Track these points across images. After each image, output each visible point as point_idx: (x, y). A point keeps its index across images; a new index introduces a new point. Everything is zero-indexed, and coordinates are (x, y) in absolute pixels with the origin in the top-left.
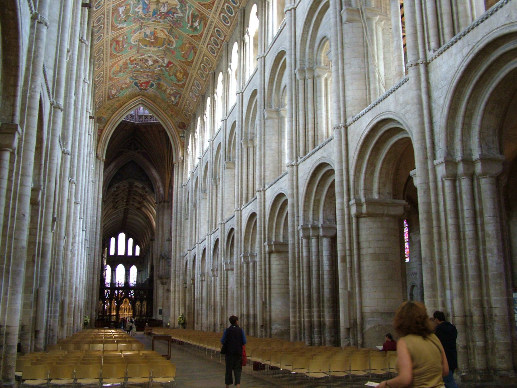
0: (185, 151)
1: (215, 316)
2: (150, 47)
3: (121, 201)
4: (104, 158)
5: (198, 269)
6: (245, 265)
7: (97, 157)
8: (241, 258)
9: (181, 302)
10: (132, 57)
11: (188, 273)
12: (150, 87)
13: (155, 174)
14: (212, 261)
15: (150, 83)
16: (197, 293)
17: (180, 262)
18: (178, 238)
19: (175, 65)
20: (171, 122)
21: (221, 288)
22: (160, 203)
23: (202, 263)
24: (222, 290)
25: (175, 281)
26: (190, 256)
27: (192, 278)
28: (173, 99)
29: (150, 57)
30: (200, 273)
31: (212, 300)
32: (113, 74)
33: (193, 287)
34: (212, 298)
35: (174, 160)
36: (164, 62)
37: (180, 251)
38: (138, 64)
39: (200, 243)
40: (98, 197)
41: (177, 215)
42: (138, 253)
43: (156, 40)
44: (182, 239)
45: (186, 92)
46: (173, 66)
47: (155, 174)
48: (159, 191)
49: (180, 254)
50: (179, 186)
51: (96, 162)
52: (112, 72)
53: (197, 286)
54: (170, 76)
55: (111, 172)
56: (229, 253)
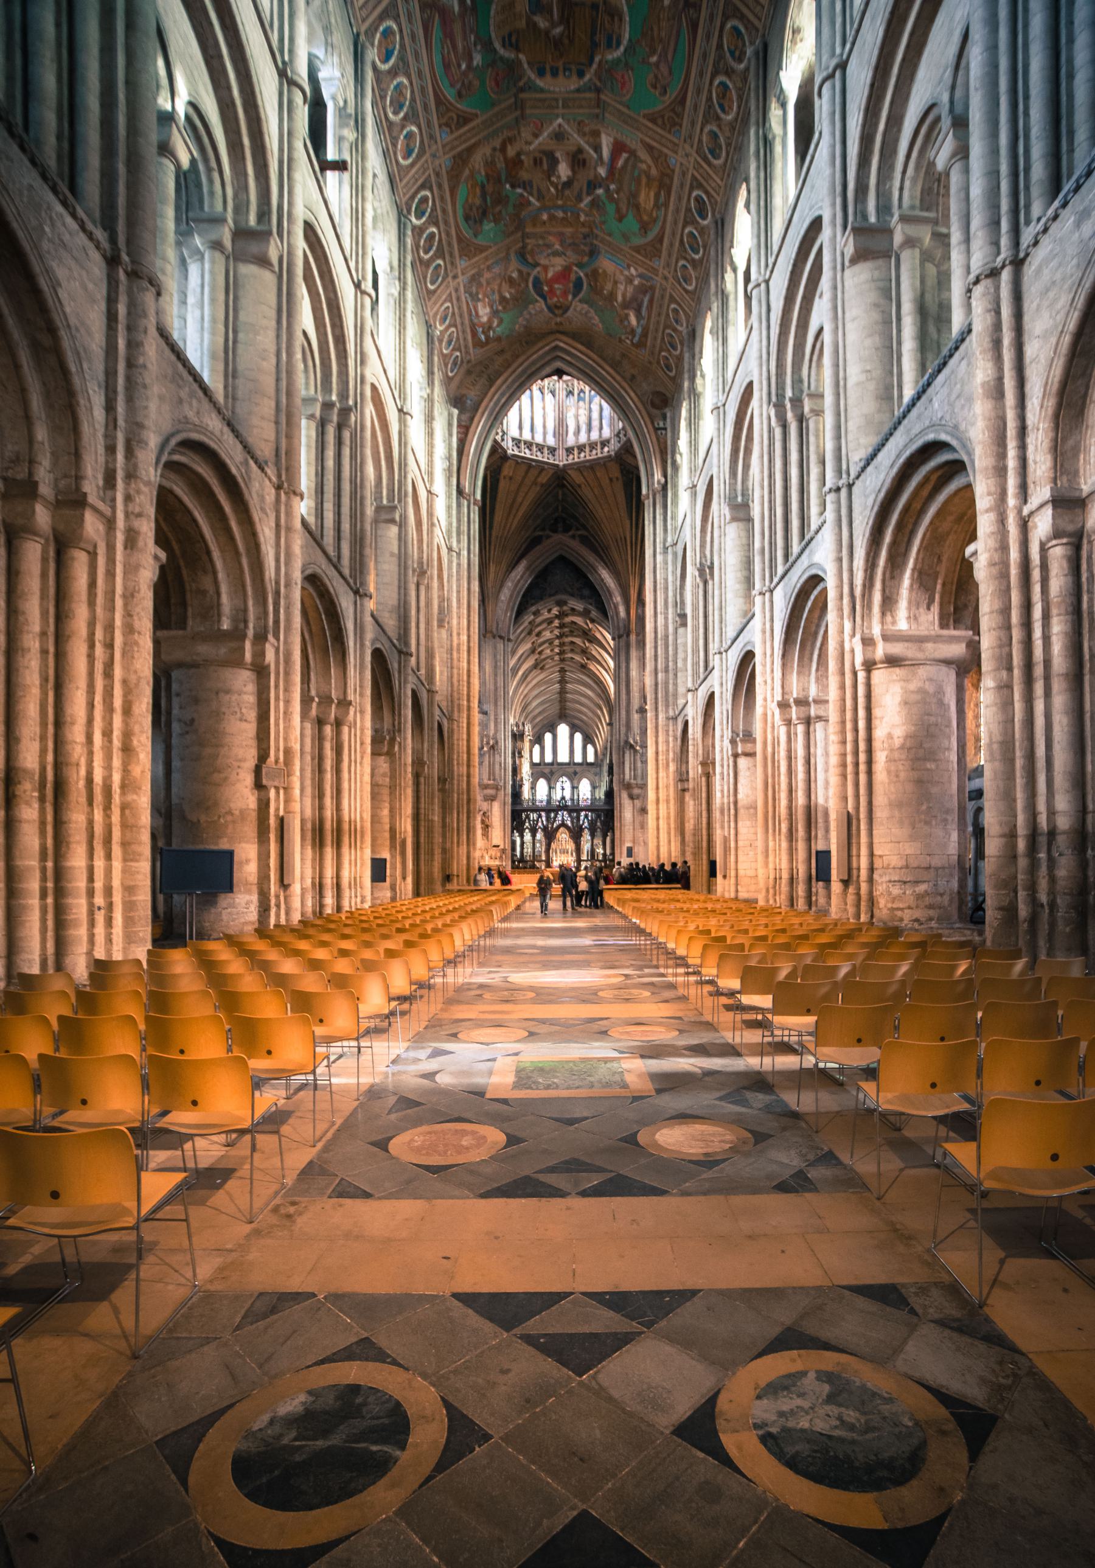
0: (669, 461)
1: (791, 851)
2: (555, 73)
3: (548, 651)
4: (479, 497)
5: (722, 724)
6: (1058, 553)
7: (460, 492)
8: (1024, 525)
9: (672, 826)
10: (511, 140)
11: (691, 748)
12: (575, 296)
13: (607, 577)
14: (778, 674)
15: (573, 277)
16: (722, 791)
17: (667, 731)
18: (660, 675)
19: (633, 153)
20: (632, 394)
21: (844, 742)
22: (620, 637)
23: (733, 705)
24: (849, 747)
25: (657, 778)
26: (695, 704)
27: (700, 759)
28: (633, 320)
29: (559, 136)
30: (728, 734)
31: (784, 802)
32: (467, 218)
33: (704, 784)
34: (783, 796)
35: (644, 491)
36: (601, 157)
37: (667, 706)
38: (530, 183)
39: (726, 651)
40: (469, 589)
41: (656, 622)
42: (591, 758)
43: (568, 23)
44: (671, 675)
45: (666, 272)
46: (627, 161)
47: (607, 577)
48: (617, 613)
49: (667, 711)
50: (658, 550)
51: (459, 505)
52: (460, 212)
53: (722, 773)
54: (620, 218)
55: (519, 581)
56: (877, 597)
